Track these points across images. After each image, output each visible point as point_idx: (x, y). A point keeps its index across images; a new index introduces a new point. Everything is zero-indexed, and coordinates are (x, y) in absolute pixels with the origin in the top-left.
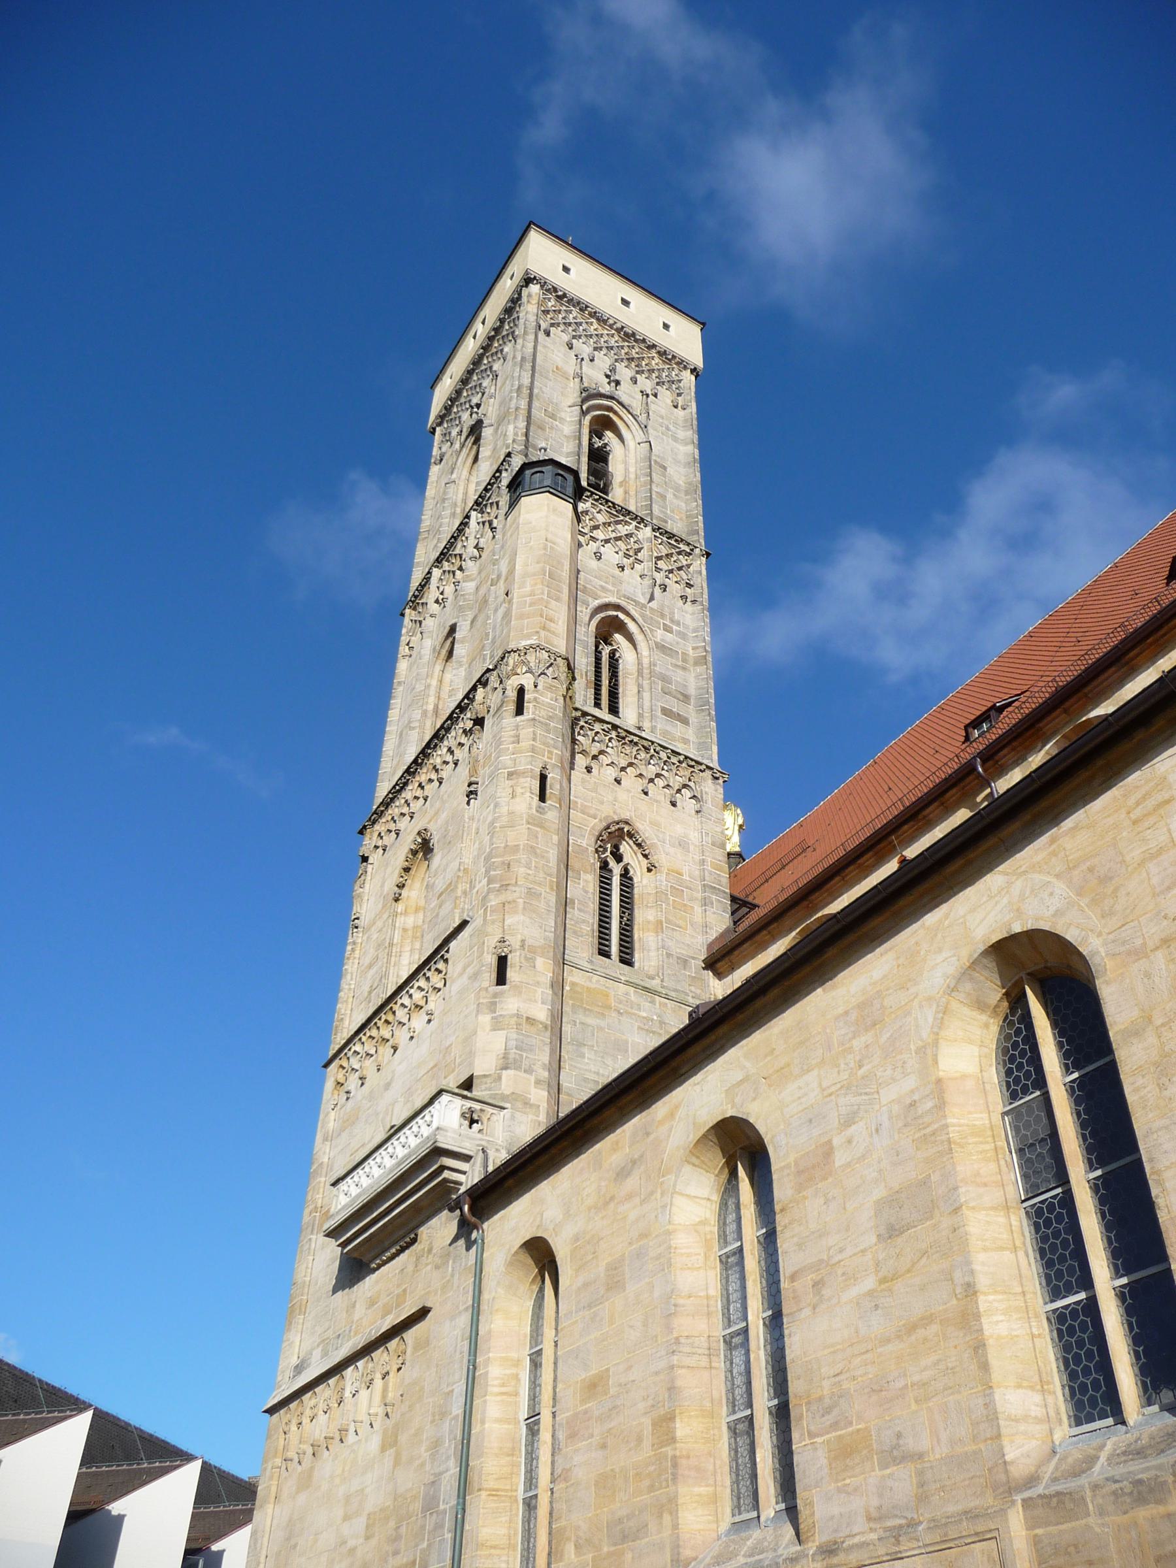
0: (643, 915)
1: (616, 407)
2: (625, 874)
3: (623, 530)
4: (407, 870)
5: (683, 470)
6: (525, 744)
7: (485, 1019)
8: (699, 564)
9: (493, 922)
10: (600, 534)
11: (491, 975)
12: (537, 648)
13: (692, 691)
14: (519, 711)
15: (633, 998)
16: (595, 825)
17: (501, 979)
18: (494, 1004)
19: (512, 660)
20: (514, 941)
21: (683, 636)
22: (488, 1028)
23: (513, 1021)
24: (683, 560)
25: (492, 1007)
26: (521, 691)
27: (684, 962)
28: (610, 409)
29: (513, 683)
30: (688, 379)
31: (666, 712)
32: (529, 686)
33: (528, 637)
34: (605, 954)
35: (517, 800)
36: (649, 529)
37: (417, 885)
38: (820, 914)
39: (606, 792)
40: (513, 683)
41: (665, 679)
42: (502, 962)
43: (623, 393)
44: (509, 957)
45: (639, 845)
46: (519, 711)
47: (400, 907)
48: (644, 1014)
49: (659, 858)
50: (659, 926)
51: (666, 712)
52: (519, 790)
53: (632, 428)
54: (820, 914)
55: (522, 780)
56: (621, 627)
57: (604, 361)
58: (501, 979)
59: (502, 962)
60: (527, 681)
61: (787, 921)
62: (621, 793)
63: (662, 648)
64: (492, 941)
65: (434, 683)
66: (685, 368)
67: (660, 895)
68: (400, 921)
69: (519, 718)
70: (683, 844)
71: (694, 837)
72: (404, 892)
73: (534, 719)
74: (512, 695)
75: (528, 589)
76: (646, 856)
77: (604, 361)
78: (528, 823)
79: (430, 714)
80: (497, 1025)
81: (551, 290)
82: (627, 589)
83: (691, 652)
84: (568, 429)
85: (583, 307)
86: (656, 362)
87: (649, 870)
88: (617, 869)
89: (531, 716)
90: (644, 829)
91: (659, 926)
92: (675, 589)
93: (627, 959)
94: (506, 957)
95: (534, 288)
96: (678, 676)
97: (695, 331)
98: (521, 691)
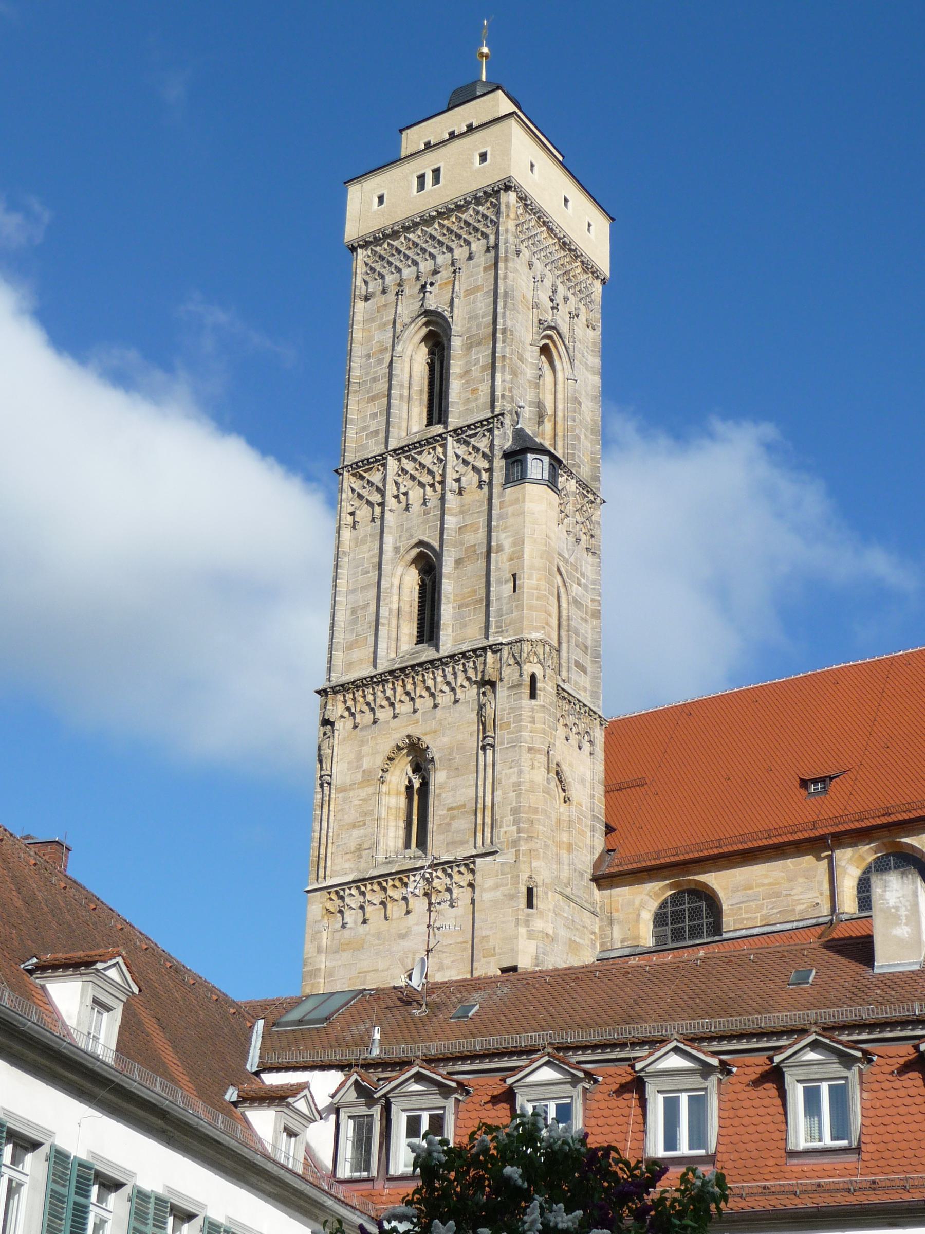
1: (556, 338)
4: (391, 759)
5: (590, 404)
6: (539, 726)
7: (522, 930)
9: (524, 862)
11: (523, 901)
13: (589, 643)
14: (533, 695)
15: (561, 903)
17: (530, 905)
18: (528, 921)
20: (539, 879)
22: (525, 937)
23: (540, 935)
25: (527, 923)
26: (533, 677)
27: (581, 875)
28: (550, 337)
30: (598, 287)
32: (539, 676)
33: (537, 629)
35: (535, 771)
36: (574, 481)
37: (397, 772)
38: (691, 878)
40: (528, 669)
42: (530, 891)
44: (535, 889)
45: (561, 782)
46: (533, 695)
47: (384, 788)
48: (566, 915)
52: (536, 764)
53: (564, 359)
54: (691, 878)
55: (538, 756)
58: (530, 905)
59: (530, 891)
60: (538, 671)
61: (665, 873)
64: (524, 877)
65: (396, 582)
66: (597, 277)
68: (385, 800)
69: (533, 702)
72: (388, 776)
73: (544, 706)
74: (527, 679)
75: (535, 582)
76: (564, 791)
78: (544, 792)
79: (395, 612)
80: (531, 936)
83: (590, 604)
87: (565, 802)
89: (542, 703)
94: (532, 889)
95: (512, 197)
97: (602, 225)
98: (533, 677)
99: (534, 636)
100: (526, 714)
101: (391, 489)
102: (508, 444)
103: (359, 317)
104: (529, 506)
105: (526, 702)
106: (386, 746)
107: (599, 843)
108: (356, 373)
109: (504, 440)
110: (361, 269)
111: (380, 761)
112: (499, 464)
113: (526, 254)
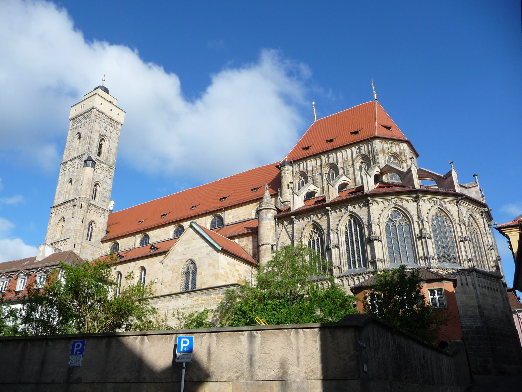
0: (93, 234)
2: (92, 228)
3: (102, 165)
5: (115, 149)
8: (113, 171)
10: (98, 167)
12: (85, 197)
16: (89, 221)
19: (81, 199)
21: (108, 186)
24: (111, 170)
29: (81, 203)
31: (103, 201)
34: (87, 239)
39: (92, 216)
40: (81, 203)
41: (103, 194)
43: (107, 134)
49: (97, 226)
50: (95, 236)
51: (103, 201)
56: (98, 184)
57: (105, 125)
62: (94, 216)
63: (104, 188)
67: (96, 231)
70: (101, 223)
71: (103, 222)
77: (105, 125)
81: (97, 110)
82: (100, 178)
84: (96, 144)
85: (103, 113)
86: (115, 124)
88: (91, 227)
90: (96, 221)
91: (95, 236)
92: (108, 176)
93: (90, 240)
95: (95, 110)
96: (105, 194)
99: (83, 196)
100: (79, 211)
101: (68, 168)
102: (85, 159)
103: (69, 134)
104: (86, 171)
105: (80, 209)
106: (59, 218)
107: (104, 235)
108: (67, 145)
109: (85, 158)
110: (71, 124)
111: (57, 221)
112: (83, 163)
113: (98, 121)
